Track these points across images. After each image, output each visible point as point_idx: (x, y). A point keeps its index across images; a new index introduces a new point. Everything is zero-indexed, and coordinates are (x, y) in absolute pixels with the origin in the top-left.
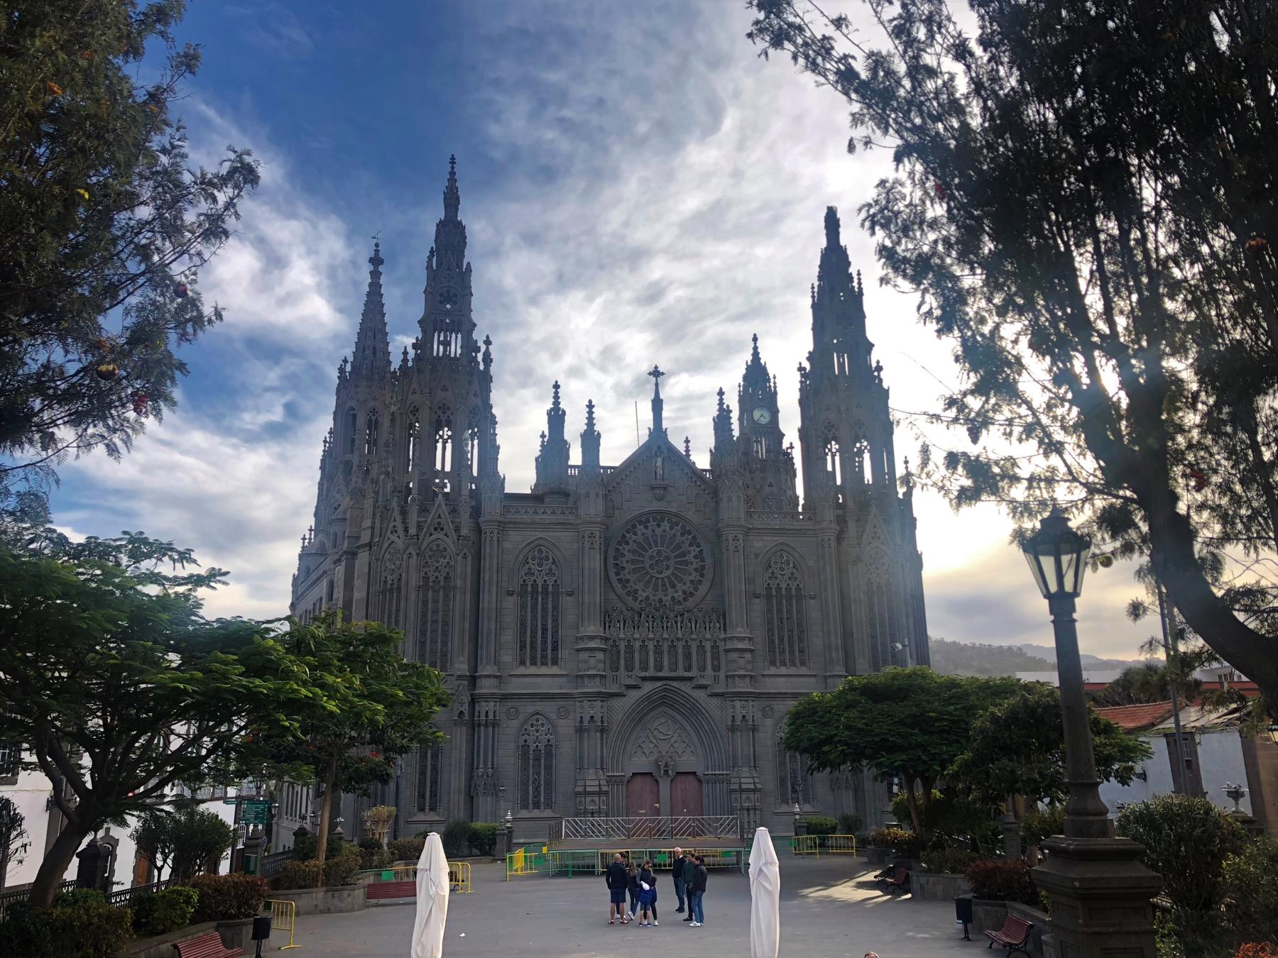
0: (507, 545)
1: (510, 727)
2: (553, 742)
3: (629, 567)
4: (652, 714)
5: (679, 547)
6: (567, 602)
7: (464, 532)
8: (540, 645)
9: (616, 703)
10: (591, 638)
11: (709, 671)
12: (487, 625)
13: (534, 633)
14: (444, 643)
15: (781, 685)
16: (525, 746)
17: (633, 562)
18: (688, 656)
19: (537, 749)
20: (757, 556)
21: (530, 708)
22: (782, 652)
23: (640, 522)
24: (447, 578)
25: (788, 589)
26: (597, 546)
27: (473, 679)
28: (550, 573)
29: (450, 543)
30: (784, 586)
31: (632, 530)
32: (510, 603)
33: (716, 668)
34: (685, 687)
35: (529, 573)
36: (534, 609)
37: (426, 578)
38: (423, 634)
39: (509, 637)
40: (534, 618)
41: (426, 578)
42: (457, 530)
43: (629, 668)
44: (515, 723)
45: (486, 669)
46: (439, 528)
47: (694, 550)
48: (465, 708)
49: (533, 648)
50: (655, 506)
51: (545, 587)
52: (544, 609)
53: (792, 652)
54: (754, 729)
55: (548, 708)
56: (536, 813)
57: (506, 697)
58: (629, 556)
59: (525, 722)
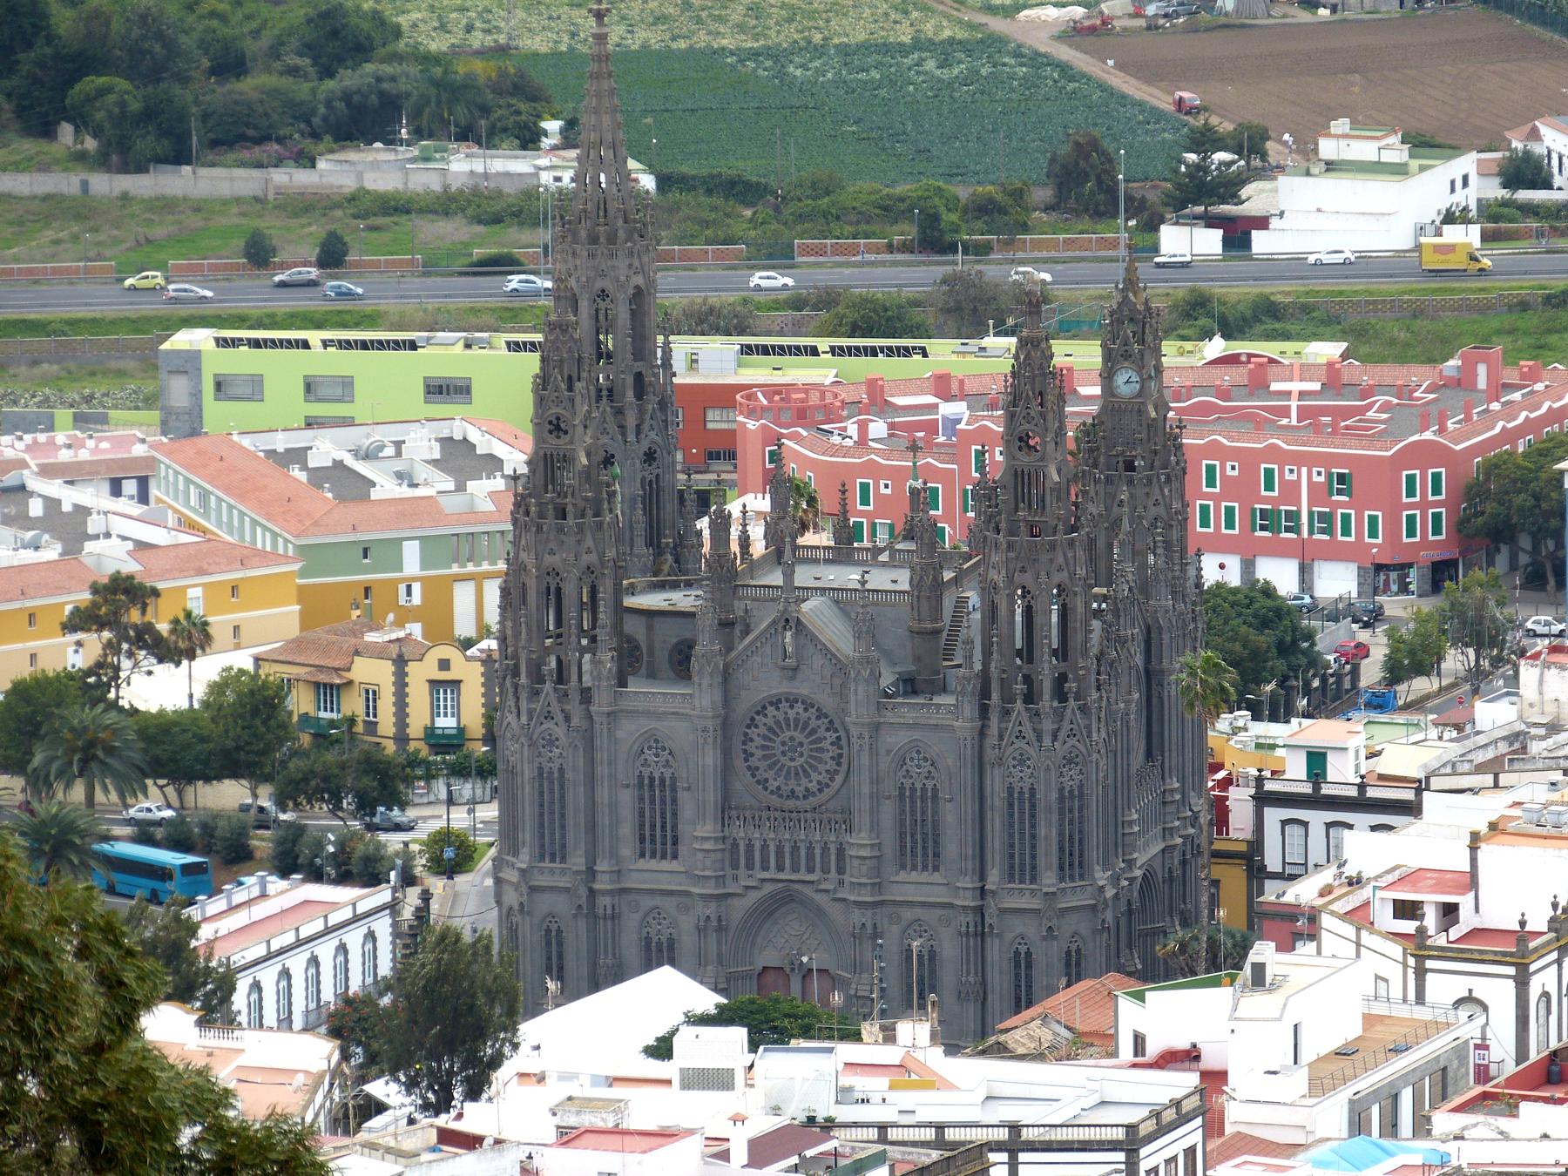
0: (620, 734)
1: (631, 921)
2: (675, 936)
3: (759, 753)
4: (783, 909)
6: (683, 796)
7: (575, 722)
8: (659, 836)
9: (735, 901)
11: (833, 874)
12: (604, 820)
13: (653, 827)
14: (563, 836)
15: (911, 894)
16: (648, 940)
17: (763, 747)
19: (659, 943)
20: (889, 752)
21: (648, 902)
22: (914, 855)
23: (771, 704)
24: (561, 770)
25: (924, 789)
26: (710, 740)
27: (591, 873)
29: (560, 732)
30: (918, 786)
31: (762, 711)
32: (627, 797)
34: (808, 891)
35: (646, 763)
36: (652, 802)
37: (540, 769)
38: (542, 826)
39: (627, 830)
40: (653, 810)
41: (540, 769)
42: (567, 719)
43: (750, 866)
44: (637, 917)
45: (601, 866)
46: (549, 716)
48: (583, 901)
49: (653, 841)
51: (662, 781)
52: (663, 802)
53: (925, 854)
55: (669, 904)
59: (647, 915)
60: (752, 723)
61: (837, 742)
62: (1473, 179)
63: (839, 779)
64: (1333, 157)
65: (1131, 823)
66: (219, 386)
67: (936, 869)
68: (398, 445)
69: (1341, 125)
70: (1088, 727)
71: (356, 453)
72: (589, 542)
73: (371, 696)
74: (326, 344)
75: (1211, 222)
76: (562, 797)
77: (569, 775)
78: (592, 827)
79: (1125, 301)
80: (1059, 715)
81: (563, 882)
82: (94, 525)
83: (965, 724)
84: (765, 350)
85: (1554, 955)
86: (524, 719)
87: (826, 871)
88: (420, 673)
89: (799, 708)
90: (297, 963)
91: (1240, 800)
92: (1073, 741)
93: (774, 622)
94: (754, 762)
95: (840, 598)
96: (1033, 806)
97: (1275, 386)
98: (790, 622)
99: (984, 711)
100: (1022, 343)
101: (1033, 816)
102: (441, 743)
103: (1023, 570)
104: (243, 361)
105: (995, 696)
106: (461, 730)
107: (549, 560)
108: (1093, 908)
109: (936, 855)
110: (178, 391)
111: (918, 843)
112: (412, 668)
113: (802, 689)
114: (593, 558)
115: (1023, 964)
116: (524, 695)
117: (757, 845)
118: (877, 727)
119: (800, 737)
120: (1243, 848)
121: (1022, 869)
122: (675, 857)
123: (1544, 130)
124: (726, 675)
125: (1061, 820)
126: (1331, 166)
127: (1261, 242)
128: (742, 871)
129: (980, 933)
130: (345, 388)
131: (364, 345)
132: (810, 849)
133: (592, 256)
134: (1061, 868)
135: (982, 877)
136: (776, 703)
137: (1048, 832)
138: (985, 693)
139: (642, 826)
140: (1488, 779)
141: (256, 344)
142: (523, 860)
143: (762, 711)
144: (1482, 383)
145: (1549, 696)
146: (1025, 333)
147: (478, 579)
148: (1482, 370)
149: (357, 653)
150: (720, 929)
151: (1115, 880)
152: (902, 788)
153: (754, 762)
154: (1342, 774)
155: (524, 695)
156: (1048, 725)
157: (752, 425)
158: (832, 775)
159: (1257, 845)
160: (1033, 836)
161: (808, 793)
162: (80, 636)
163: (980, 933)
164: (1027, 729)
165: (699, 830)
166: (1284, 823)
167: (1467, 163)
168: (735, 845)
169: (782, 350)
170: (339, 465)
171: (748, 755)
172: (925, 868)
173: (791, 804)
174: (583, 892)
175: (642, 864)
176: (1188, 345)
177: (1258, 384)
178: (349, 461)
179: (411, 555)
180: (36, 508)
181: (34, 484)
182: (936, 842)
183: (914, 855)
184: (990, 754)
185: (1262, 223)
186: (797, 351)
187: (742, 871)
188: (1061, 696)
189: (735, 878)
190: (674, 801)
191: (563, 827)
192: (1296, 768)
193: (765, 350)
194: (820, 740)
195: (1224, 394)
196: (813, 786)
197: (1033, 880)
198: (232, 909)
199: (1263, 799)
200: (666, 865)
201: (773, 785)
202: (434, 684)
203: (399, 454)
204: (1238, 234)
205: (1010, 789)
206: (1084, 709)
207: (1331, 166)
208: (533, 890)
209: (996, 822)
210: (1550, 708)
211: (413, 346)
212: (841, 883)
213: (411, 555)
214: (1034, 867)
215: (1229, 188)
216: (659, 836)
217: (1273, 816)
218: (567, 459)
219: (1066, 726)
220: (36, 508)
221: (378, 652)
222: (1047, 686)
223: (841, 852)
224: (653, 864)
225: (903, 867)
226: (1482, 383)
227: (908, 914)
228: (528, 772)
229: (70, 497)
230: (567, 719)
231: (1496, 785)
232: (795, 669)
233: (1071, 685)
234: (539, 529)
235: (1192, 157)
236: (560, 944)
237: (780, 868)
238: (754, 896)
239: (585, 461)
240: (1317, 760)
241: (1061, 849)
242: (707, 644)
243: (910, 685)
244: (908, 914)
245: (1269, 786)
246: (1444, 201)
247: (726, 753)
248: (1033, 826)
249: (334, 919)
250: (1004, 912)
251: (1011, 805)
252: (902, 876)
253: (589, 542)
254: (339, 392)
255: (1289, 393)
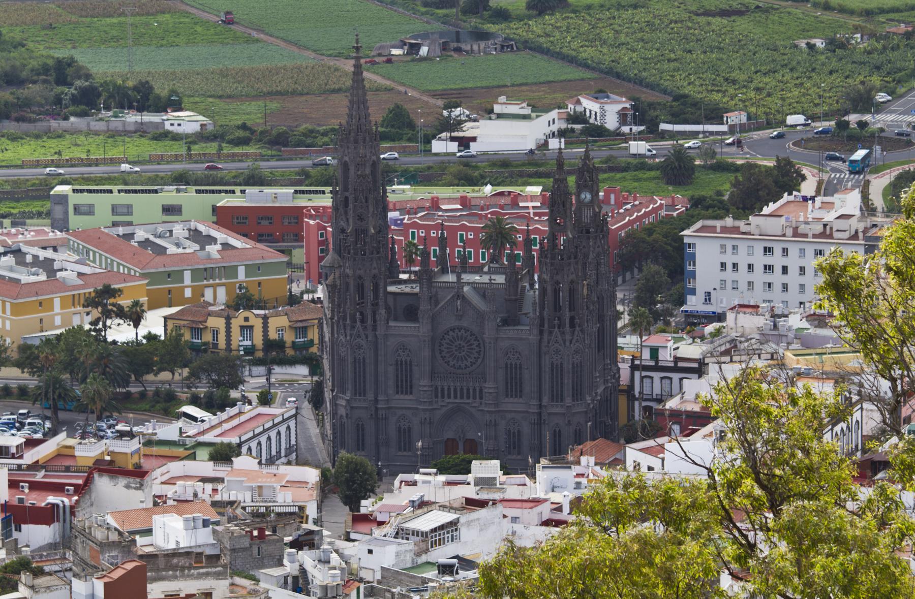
0: (389, 343)
5: (469, 341)
6: (415, 369)
7: (370, 338)
8: (405, 385)
10: (425, 386)
11: (478, 400)
13: (402, 381)
14: (364, 386)
15: (510, 407)
16: (400, 428)
18: (468, 393)
19: (404, 429)
22: (512, 391)
24: (364, 358)
25: (516, 364)
27: (376, 401)
28: (408, 355)
29: (363, 343)
31: (447, 333)
32: (391, 369)
33: (481, 398)
35: (399, 355)
36: (402, 371)
37: (355, 358)
38: (355, 381)
39: (391, 383)
40: (402, 374)
41: (355, 358)
42: (367, 337)
43: (443, 397)
46: (359, 336)
47: (476, 343)
48: (373, 412)
50: (457, 324)
51: (406, 362)
52: (406, 371)
54: (496, 425)
56: (405, 453)
57: (389, 408)
58: (446, 346)
60: (443, 338)
61: (479, 346)
62: (556, 121)
63: (480, 361)
64: (500, 112)
65: (596, 377)
66: (75, 209)
67: (521, 397)
68: (171, 231)
69: (502, 99)
70: (584, 338)
71: (155, 236)
72: (375, 265)
73: (215, 333)
74: (119, 191)
75: (453, 139)
76: (364, 370)
77: (367, 361)
78: (377, 382)
79: (585, 164)
80: (573, 333)
81: (364, 405)
82: (56, 266)
83: (533, 338)
84: (303, 192)
85: (830, 427)
86: (348, 338)
87: (474, 398)
88: (236, 323)
89: (463, 331)
90: (263, 439)
91: (624, 368)
92: (577, 344)
93: (453, 296)
94: (444, 354)
95: (475, 286)
96: (562, 370)
97: (521, 204)
98: (460, 296)
99: (541, 332)
100: (556, 181)
101: (562, 375)
102: (250, 351)
103: (557, 274)
104: (84, 199)
105: (546, 326)
106: (253, 346)
107: (358, 272)
108: (586, 412)
109: (521, 391)
110: (58, 211)
111: (513, 386)
112: (233, 321)
113: (465, 324)
114: (376, 271)
115: (557, 436)
116: (348, 328)
117: (446, 388)
118: (497, 339)
119: (463, 344)
120: (626, 388)
121: (557, 397)
122: (411, 393)
123: (582, 100)
124: (433, 319)
125: (573, 376)
126: (500, 116)
127: (474, 148)
128: (439, 399)
129: (539, 423)
130: (128, 209)
131: (136, 192)
132: (468, 390)
133: (356, 148)
134: (573, 396)
135: (540, 400)
136: (453, 330)
137: (568, 382)
138: (542, 325)
139: (397, 381)
140: (727, 359)
141: (90, 191)
142: (348, 396)
143: (447, 333)
144: (612, 202)
145: (739, 325)
146: (557, 177)
147: (214, 286)
148: (612, 196)
149: (209, 315)
150: (430, 423)
151: (593, 400)
152: (507, 364)
153: (444, 354)
154: (666, 357)
155: (348, 328)
156: (568, 337)
157: (312, 222)
158: (477, 359)
159: (631, 386)
160: (562, 383)
161: (466, 367)
162: (90, 309)
163: (539, 423)
164: (560, 339)
165: (422, 383)
166: (662, 378)
167: (554, 114)
168: (436, 388)
169: (310, 192)
170: (147, 240)
171: (441, 352)
172: (516, 397)
173: (460, 371)
174: (373, 409)
175: (397, 397)
176: (476, 188)
177: (515, 204)
178: (152, 238)
179: (187, 275)
180: (29, 259)
181: (25, 249)
182: (521, 386)
183: (512, 391)
184: (544, 349)
185: (474, 139)
186: (316, 192)
187: (439, 399)
188: (572, 325)
189: (437, 402)
190: (411, 370)
191: (364, 382)
192: (646, 355)
193: (303, 192)
194: (471, 345)
195: (502, 207)
196: (468, 364)
197: (562, 401)
198: (231, 418)
199: (634, 368)
200: (407, 397)
201: (452, 363)
202: (242, 327)
203: (171, 235)
204: (465, 143)
205: (552, 364)
206: (582, 331)
207: (500, 116)
208: (352, 408)
209: (546, 377)
210: (740, 330)
211: (156, 192)
212: (481, 403)
213: (187, 275)
214: (562, 396)
215: (457, 124)
216: (405, 385)
217: (637, 374)
218: (365, 231)
219: (575, 338)
220: (29, 259)
221: (217, 314)
222: (568, 321)
223: (481, 391)
224: (402, 397)
225: (507, 396)
226: (612, 202)
227: (509, 416)
228: (350, 359)
229: (42, 254)
230: (367, 337)
231: (731, 361)
232: (461, 316)
233: (577, 321)
234: (355, 260)
235: (445, 113)
236: (363, 430)
237: (455, 397)
238: (445, 409)
239: (373, 231)
240: (654, 352)
241: (573, 388)
242: (424, 306)
243: (506, 322)
244: (509, 416)
245: (637, 362)
246: (548, 130)
247: (433, 351)
248: (562, 379)
249: (276, 421)
250: (549, 414)
251: (552, 371)
252: (507, 400)
253: (375, 265)
254: (125, 210)
255: (527, 208)
